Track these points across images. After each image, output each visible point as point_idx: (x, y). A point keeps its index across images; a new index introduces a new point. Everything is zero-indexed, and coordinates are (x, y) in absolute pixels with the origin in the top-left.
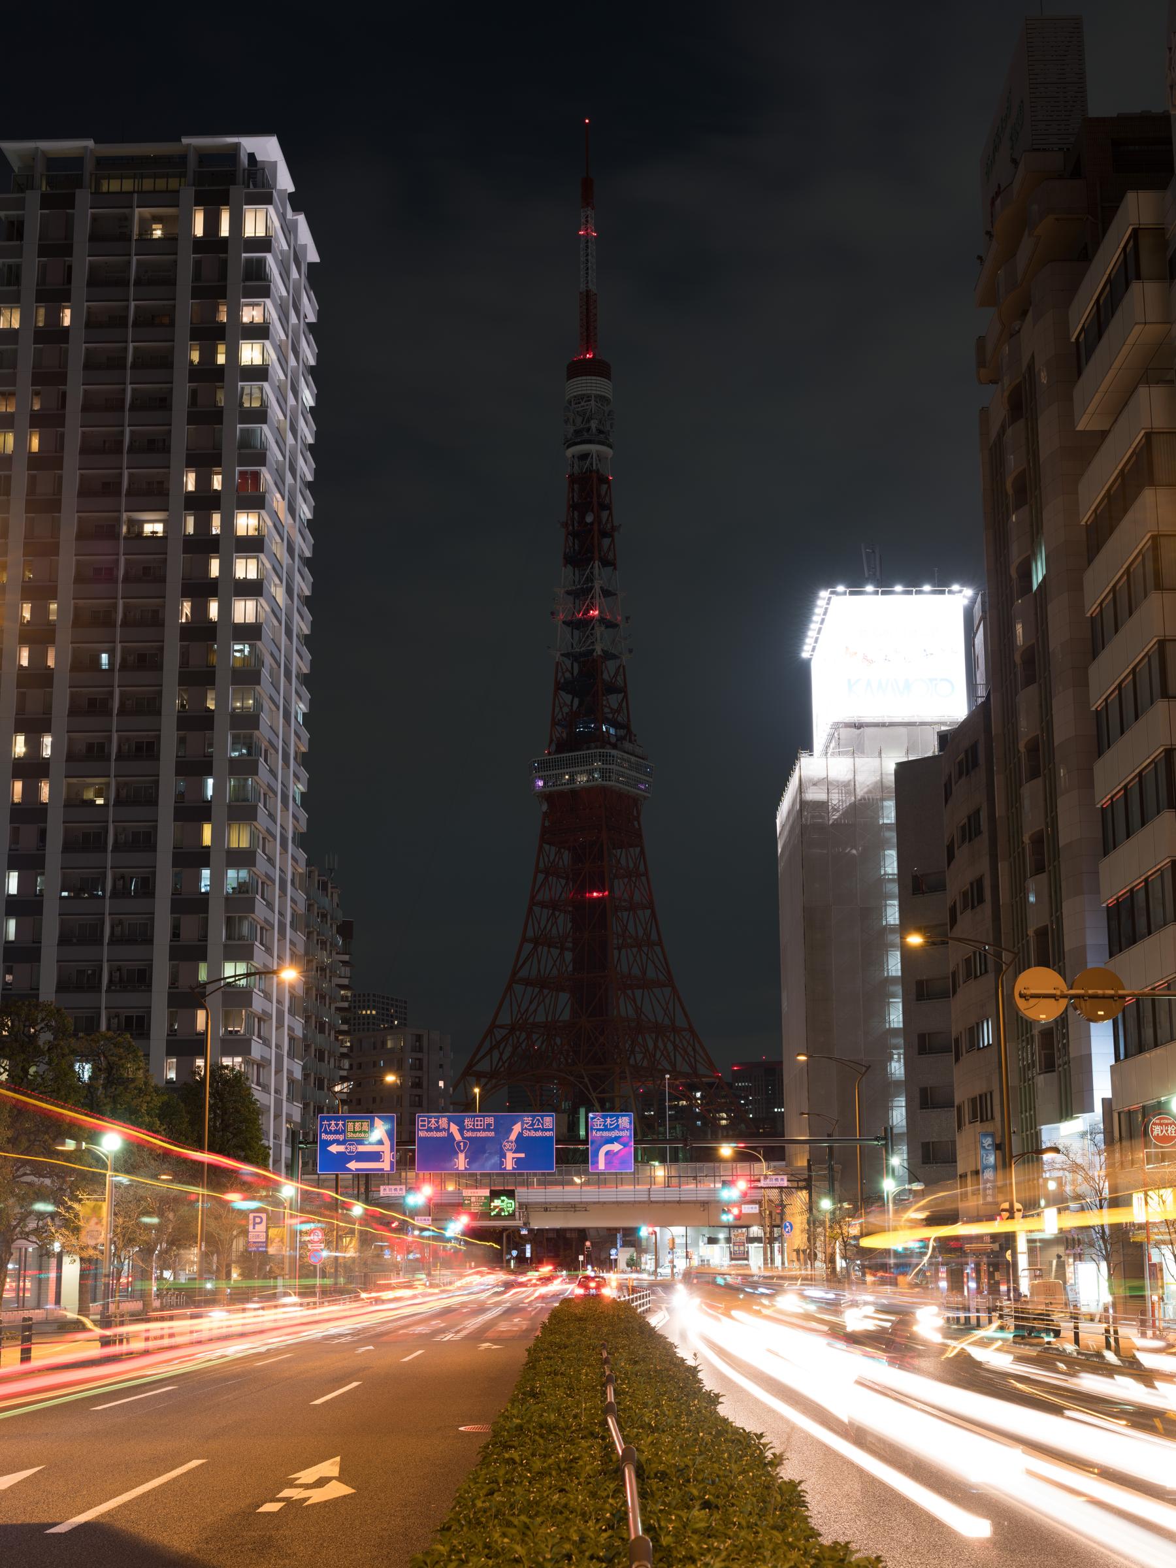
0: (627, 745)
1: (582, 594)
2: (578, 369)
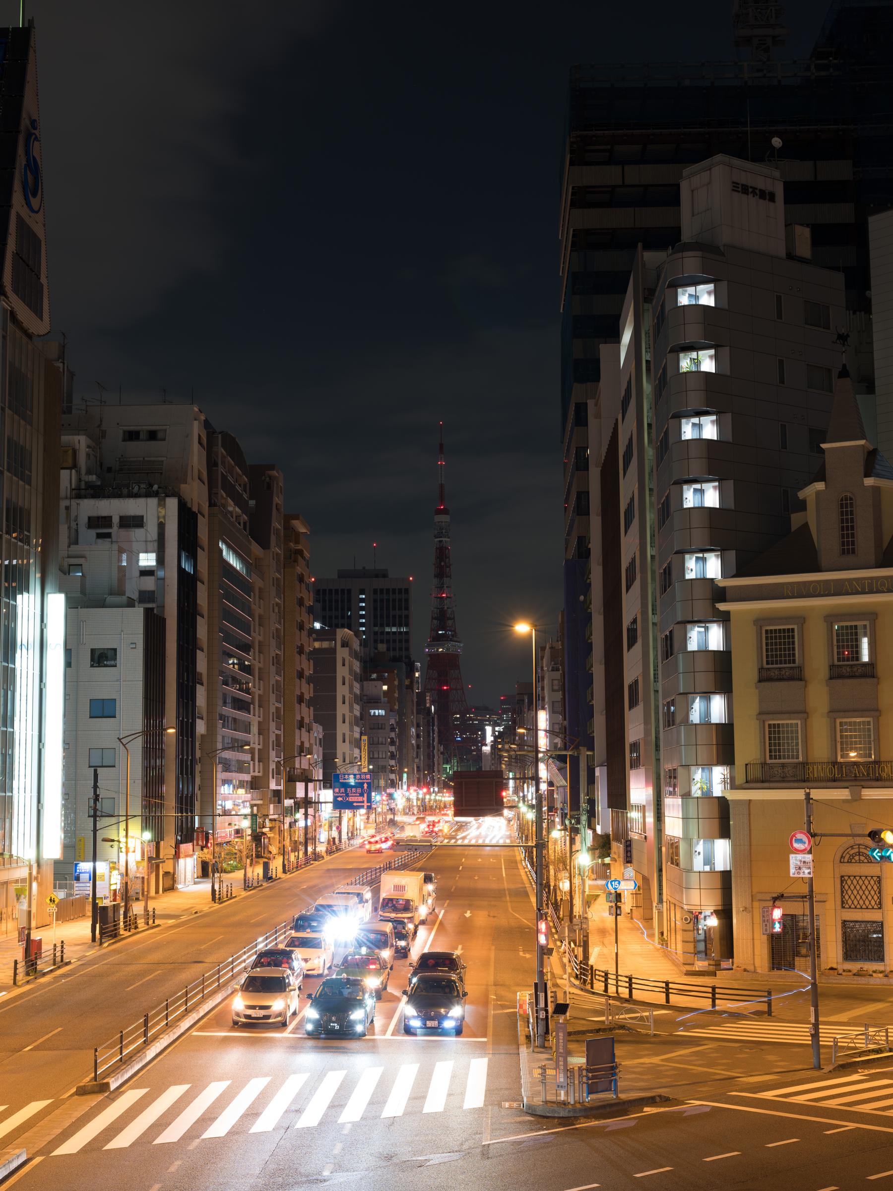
0: (455, 639)
1: (441, 588)
2: (439, 512)
